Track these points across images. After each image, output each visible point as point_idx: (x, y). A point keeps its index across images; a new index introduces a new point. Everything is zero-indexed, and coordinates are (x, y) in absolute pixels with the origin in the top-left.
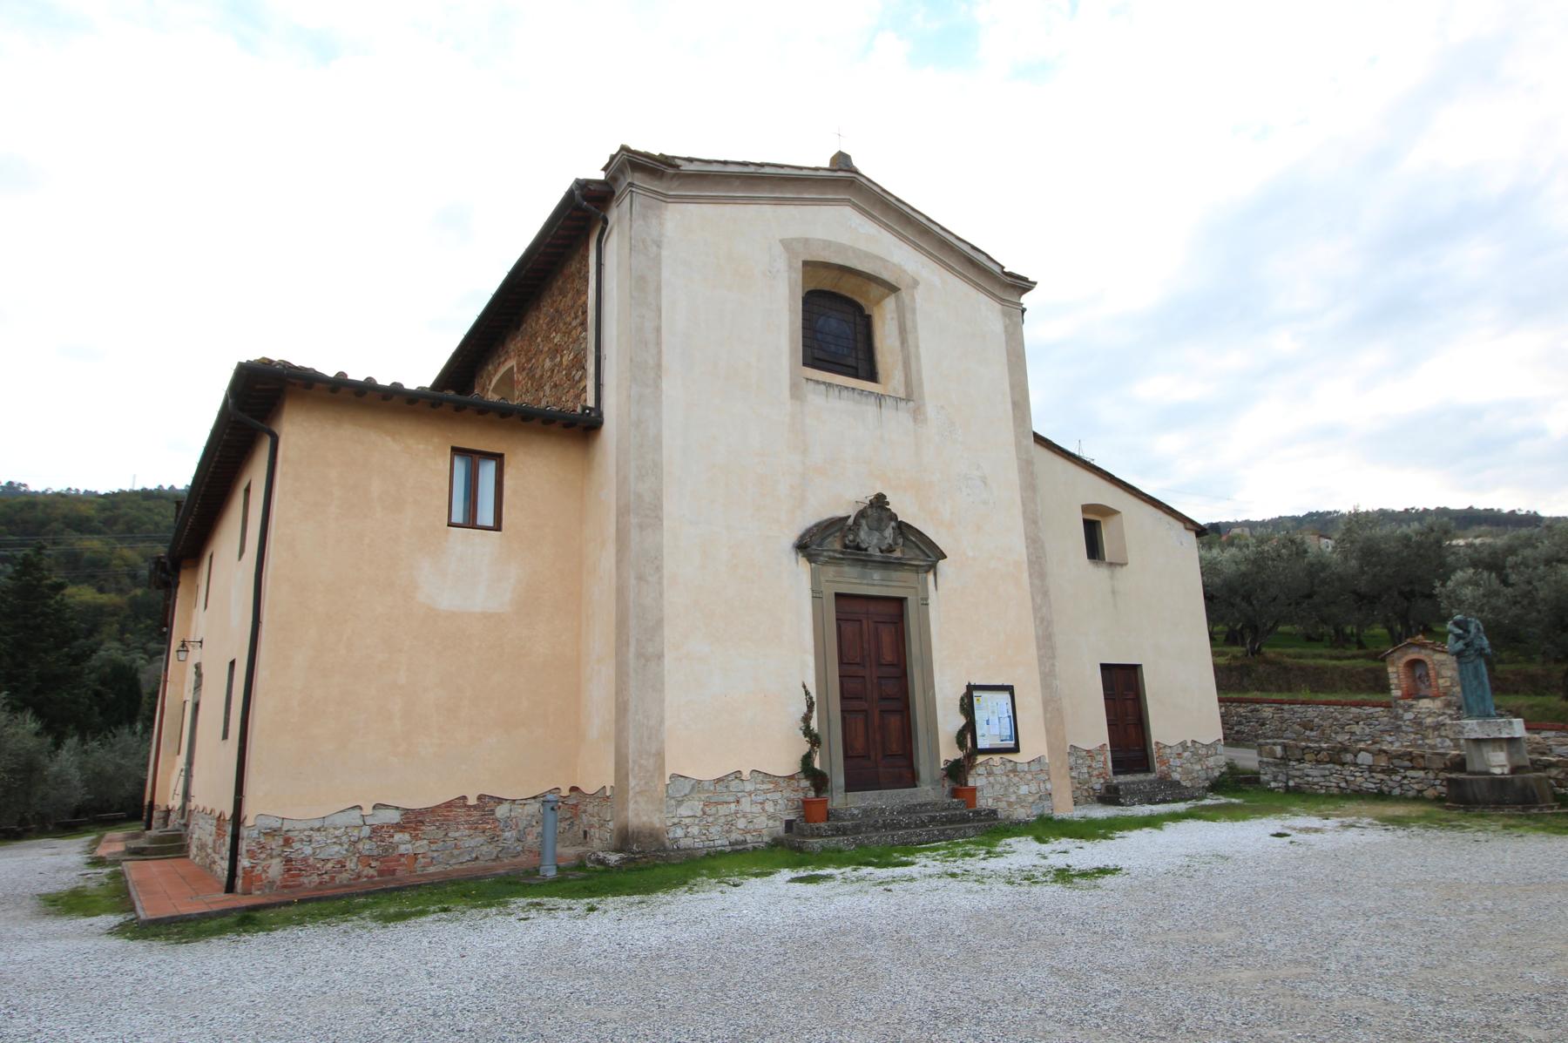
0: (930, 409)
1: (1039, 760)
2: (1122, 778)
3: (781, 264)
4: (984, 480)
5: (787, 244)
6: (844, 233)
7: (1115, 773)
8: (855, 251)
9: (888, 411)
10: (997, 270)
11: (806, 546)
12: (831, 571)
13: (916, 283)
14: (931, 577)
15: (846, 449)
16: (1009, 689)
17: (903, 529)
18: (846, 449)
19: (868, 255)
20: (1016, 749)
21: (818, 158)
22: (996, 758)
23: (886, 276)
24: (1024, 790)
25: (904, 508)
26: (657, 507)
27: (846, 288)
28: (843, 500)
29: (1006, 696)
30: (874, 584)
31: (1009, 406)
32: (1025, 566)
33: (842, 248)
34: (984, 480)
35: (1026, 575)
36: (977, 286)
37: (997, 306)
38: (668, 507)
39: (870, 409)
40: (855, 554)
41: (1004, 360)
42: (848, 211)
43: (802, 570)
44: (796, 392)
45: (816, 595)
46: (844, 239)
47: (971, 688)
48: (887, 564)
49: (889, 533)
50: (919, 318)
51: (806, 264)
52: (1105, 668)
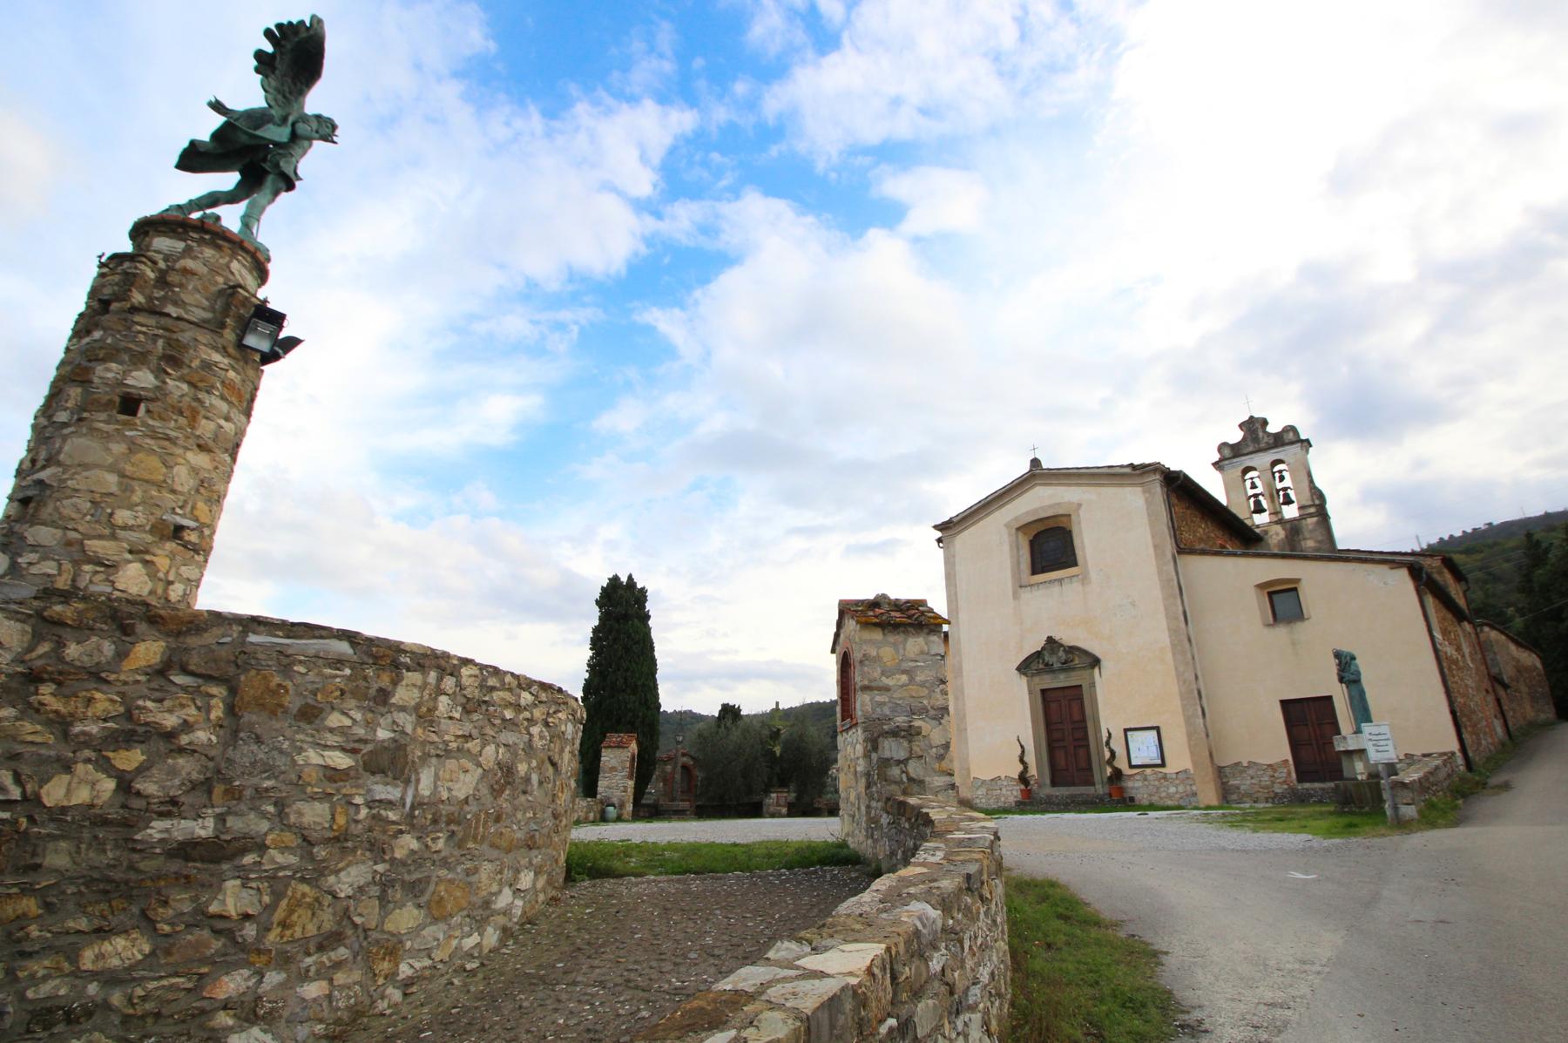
0: (1093, 575)
1: (1185, 771)
2: (1307, 785)
3: (1006, 537)
4: (1133, 604)
5: (1007, 525)
6: (1039, 501)
7: (1300, 779)
8: (1042, 508)
9: (1067, 587)
10: (1128, 470)
11: (1025, 667)
12: (1036, 679)
13: (1080, 505)
14: (1096, 670)
15: (1055, 611)
16: (1157, 729)
17: (1072, 650)
18: (1055, 611)
19: (1050, 506)
20: (1163, 765)
21: (1024, 468)
22: (1148, 771)
23: (1061, 512)
24: (1172, 790)
25: (1068, 637)
26: (960, 668)
27: (1052, 524)
28: (1035, 643)
29: (1154, 733)
30: (1062, 681)
31: (1151, 551)
32: (1169, 649)
33: (1035, 511)
34: (1133, 604)
35: (1169, 656)
36: (1121, 485)
37: (1139, 489)
38: (965, 667)
39: (1056, 589)
40: (1049, 669)
41: (1146, 520)
42: (1038, 489)
43: (1024, 680)
44: (1016, 596)
45: (1030, 692)
46: (1036, 505)
47: (1126, 731)
48: (1062, 670)
49: (1061, 653)
50: (1083, 526)
51: (1018, 529)
52: (1286, 705)
